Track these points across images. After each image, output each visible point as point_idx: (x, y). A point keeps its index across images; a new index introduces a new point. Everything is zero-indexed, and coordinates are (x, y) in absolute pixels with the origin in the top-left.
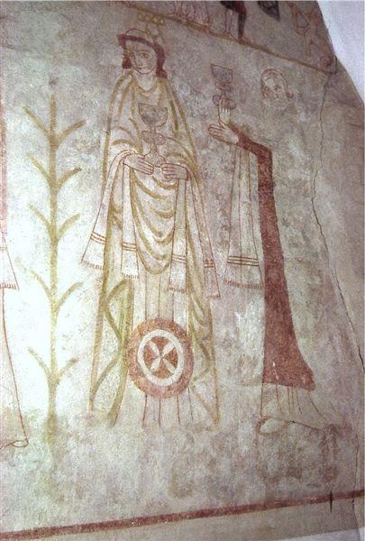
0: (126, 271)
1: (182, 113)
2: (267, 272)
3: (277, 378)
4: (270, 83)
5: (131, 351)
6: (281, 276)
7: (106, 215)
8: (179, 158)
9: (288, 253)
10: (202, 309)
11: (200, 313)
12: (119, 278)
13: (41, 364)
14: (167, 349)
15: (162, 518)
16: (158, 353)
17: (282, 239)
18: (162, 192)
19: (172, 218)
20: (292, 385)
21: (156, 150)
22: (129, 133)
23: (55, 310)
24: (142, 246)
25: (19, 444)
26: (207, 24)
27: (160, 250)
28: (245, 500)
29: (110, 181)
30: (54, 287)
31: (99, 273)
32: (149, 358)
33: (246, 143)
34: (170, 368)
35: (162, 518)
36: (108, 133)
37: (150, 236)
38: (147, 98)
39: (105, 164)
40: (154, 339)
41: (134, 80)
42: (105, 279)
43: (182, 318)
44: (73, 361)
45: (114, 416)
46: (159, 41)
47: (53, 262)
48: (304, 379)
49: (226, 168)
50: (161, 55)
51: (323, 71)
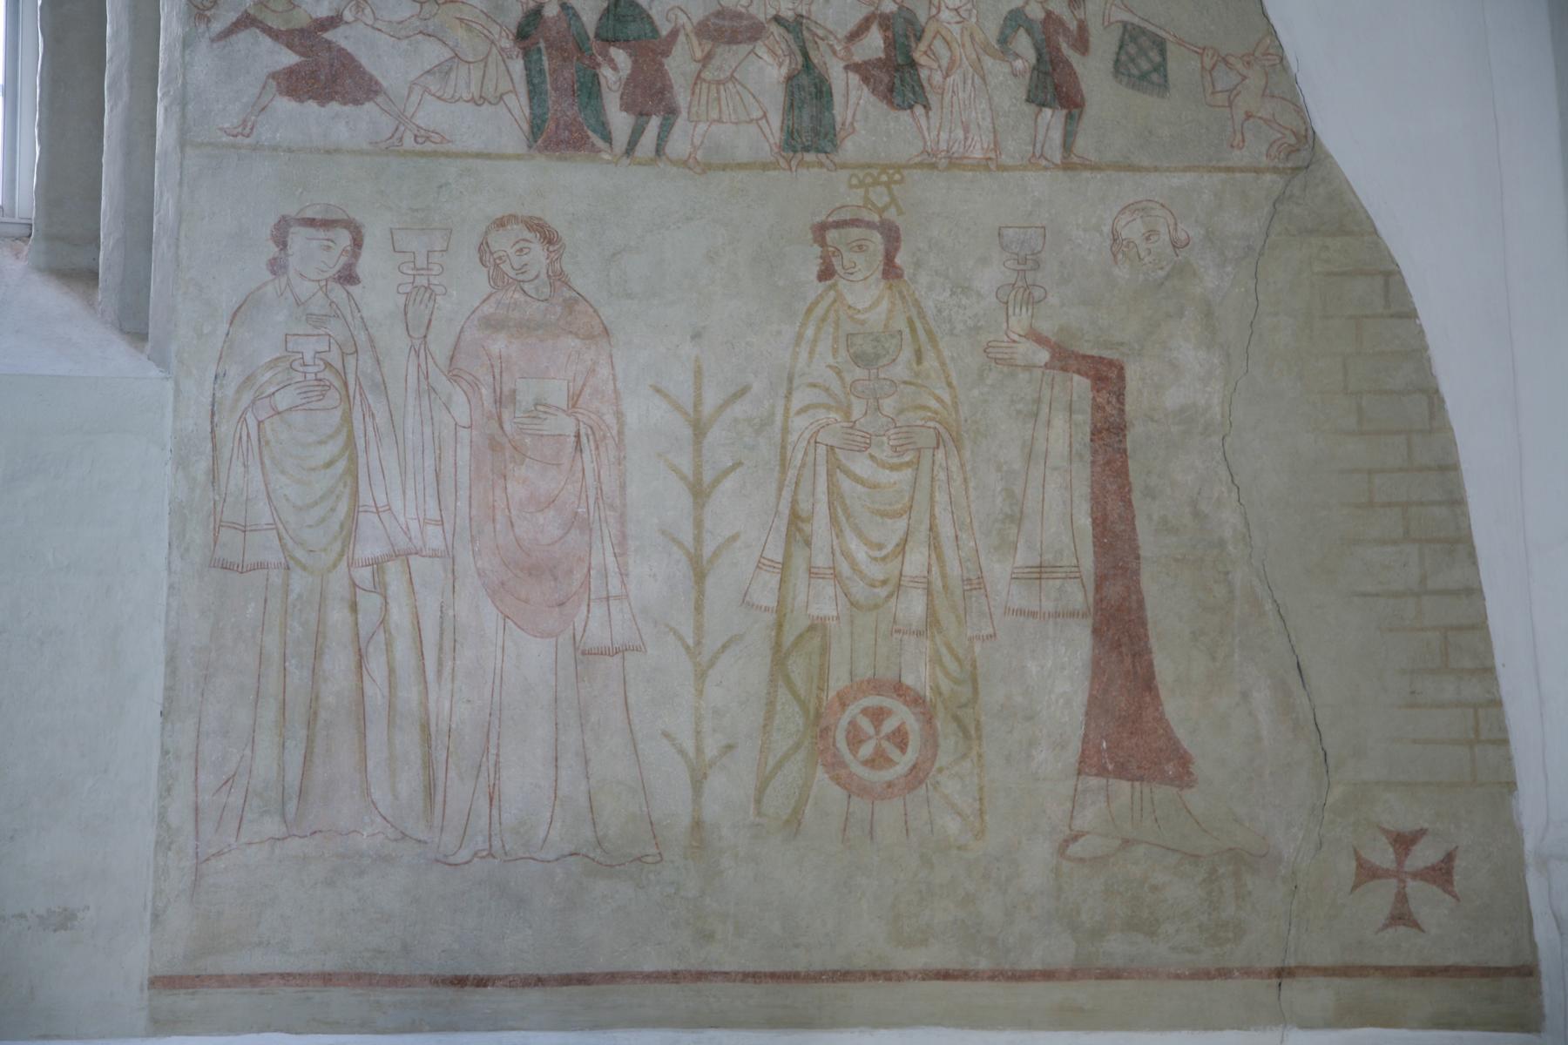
0: (814, 611)
1: (929, 333)
2: (1098, 588)
3: (1110, 767)
4: (1133, 230)
5: (826, 730)
6: (1133, 588)
7: (784, 529)
8: (921, 413)
10: (957, 659)
11: (952, 666)
12: (804, 623)
13: (682, 752)
14: (889, 725)
15: (875, 975)
16: (871, 731)
17: (1141, 523)
18: (885, 476)
19: (905, 516)
20: (1141, 779)
21: (878, 409)
22: (827, 390)
23: (701, 676)
24: (845, 568)
25: (649, 859)
26: (992, 155)
27: (876, 572)
28: (1034, 962)
29: (792, 473)
30: (698, 643)
31: (770, 618)
32: (855, 739)
33: (1064, 358)
34: (894, 753)
35: (875, 975)
36: (788, 396)
37: (861, 553)
38: (863, 323)
39: (784, 447)
40: (865, 711)
41: (840, 297)
42: (779, 626)
43: (918, 676)
44: (730, 747)
45: (793, 823)
46: (891, 214)
47: (699, 608)
48: (1170, 769)
49: (1019, 412)
50: (892, 236)
51: (1275, 170)
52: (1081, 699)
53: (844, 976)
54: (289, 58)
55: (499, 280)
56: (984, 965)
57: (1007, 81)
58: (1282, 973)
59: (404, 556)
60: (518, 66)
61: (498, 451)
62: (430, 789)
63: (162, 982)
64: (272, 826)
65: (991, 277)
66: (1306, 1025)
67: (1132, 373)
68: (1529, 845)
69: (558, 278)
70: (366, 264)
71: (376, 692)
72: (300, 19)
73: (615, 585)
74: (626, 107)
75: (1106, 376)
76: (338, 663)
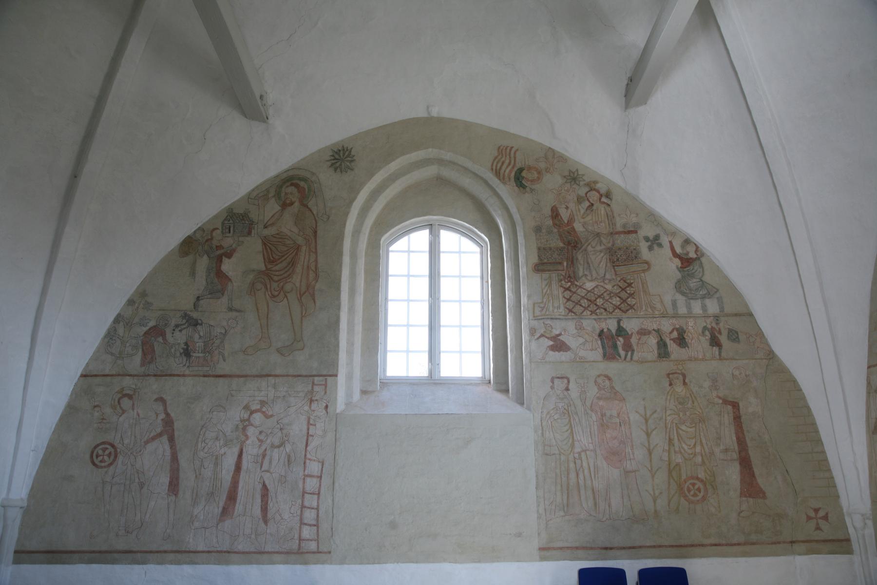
4: (737, 373)
9: (749, 444)
14: (696, 487)
18: (689, 430)
23: (653, 477)
27: (690, 451)
28: (735, 541)
32: (689, 490)
33: (726, 402)
37: (686, 447)
43: (702, 475)
50: (684, 376)
52: (739, 479)
53: (692, 546)
54: (551, 343)
55: (600, 389)
56: (724, 542)
57: (705, 341)
58: (792, 542)
59: (585, 451)
60: (599, 342)
61: (603, 426)
62: (595, 504)
63: (541, 549)
64: (562, 513)
65: (707, 384)
66: (800, 554)
67: (741, 405)
68: (845, 511)
69: (612, 388)
70: (570, 387)
71: (581, 482)
72: (553, 335)
73: (632, 456)
74: (623, 350)
75: (735, 405)
76: (573, 475)
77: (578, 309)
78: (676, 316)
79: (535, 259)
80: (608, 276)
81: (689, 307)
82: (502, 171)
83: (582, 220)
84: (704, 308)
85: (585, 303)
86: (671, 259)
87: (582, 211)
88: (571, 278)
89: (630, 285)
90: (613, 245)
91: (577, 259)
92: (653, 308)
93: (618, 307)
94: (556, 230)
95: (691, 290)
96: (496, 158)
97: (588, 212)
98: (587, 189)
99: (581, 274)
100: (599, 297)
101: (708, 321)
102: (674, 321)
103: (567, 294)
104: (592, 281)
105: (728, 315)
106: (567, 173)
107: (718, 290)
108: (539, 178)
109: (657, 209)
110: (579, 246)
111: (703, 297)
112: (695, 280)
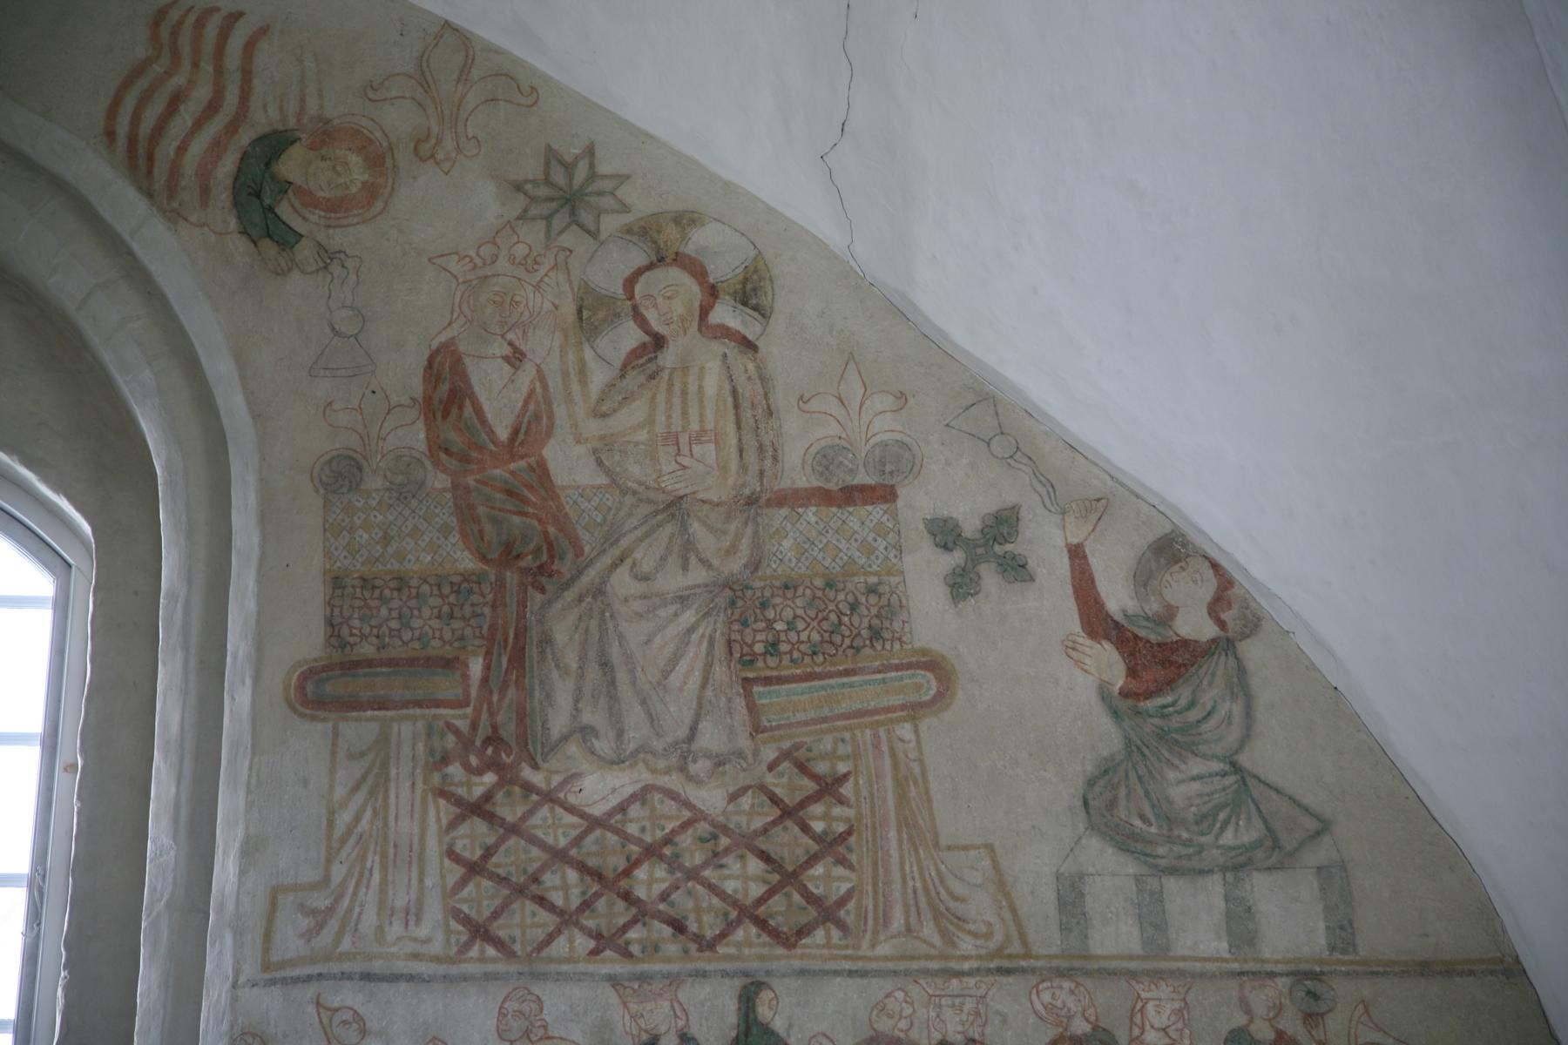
77: (525, 922)
78: (1075, 967)
79: (306, 641)
80: (711, 738)
81: (1153, 919)
82: (167, 148)
83: (593, 428)
84: (1240, 923)
85: (565, 886)
86: (1070, 647)
87: (599, 377)
88: (506, 747)
89: (829, 788)
90: (755, 565)
91: (547, 640)
92: (949, 920)
93: (750, 913)
94: (440, 481)
95: (1170, 820)
96: (138, 71)
97: (634, 379)
98: (638, 258)
99: (559, 723)
100: (651, 852)
101: (1262, 998)
102: (1063, 995)
103: (473, 836)
104: (617, 762)
105: (1374, 970)
106: (531, 168)
107: (1324, 826)
108: (371, 193)
109: (1012, 373)
110: (565, 567)
111: (1238, 865)
112: (1196, 767)
